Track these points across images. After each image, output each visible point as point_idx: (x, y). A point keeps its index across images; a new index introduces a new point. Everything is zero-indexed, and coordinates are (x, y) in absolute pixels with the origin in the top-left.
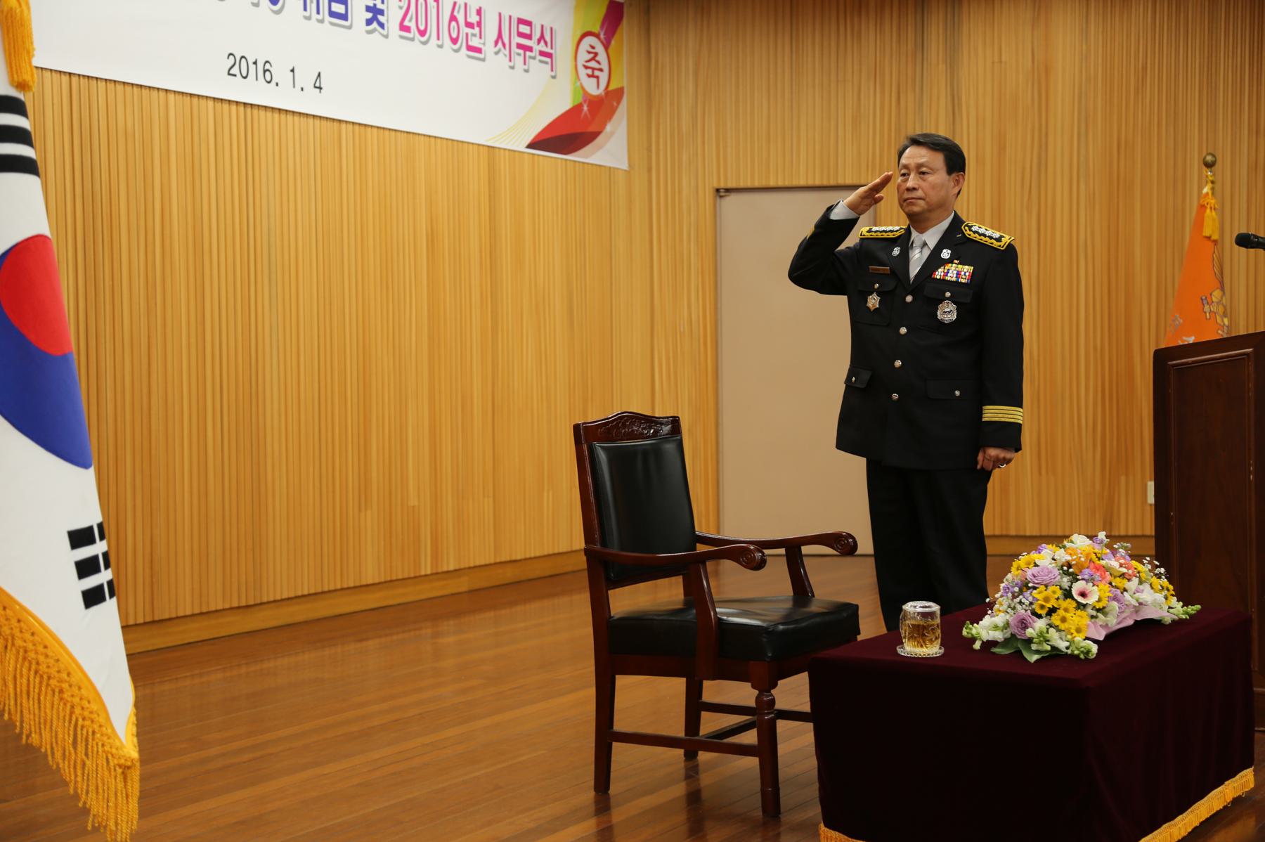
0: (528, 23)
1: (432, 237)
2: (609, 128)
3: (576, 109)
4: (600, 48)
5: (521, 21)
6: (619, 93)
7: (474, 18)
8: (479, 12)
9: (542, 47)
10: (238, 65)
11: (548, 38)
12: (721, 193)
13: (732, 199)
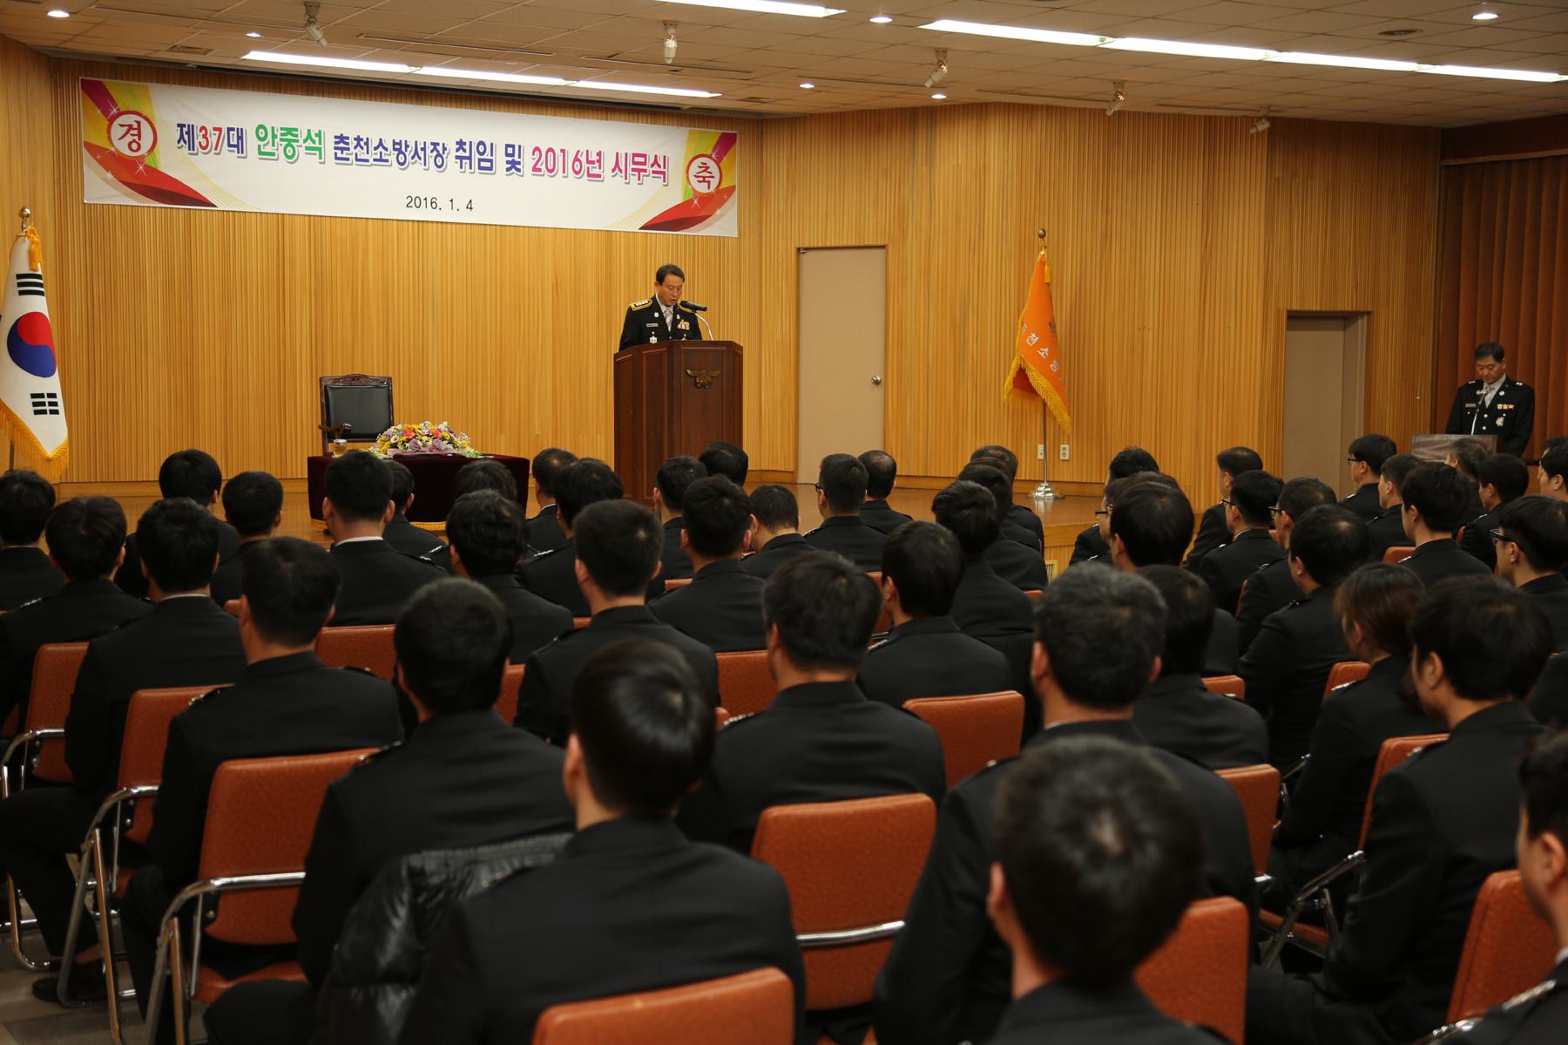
0: (644, 156)
1: (556, 286)
2: (718, 212)
3: (686, 204)
4: (711, 163)
5: (635, 155)
6: (731, 190)
7: (594, 158)
8: (599, 154)
9: (656, 168)
10: (413, 202)
11: (661, 162)
12: (800, 251)
13: (810, 254)
